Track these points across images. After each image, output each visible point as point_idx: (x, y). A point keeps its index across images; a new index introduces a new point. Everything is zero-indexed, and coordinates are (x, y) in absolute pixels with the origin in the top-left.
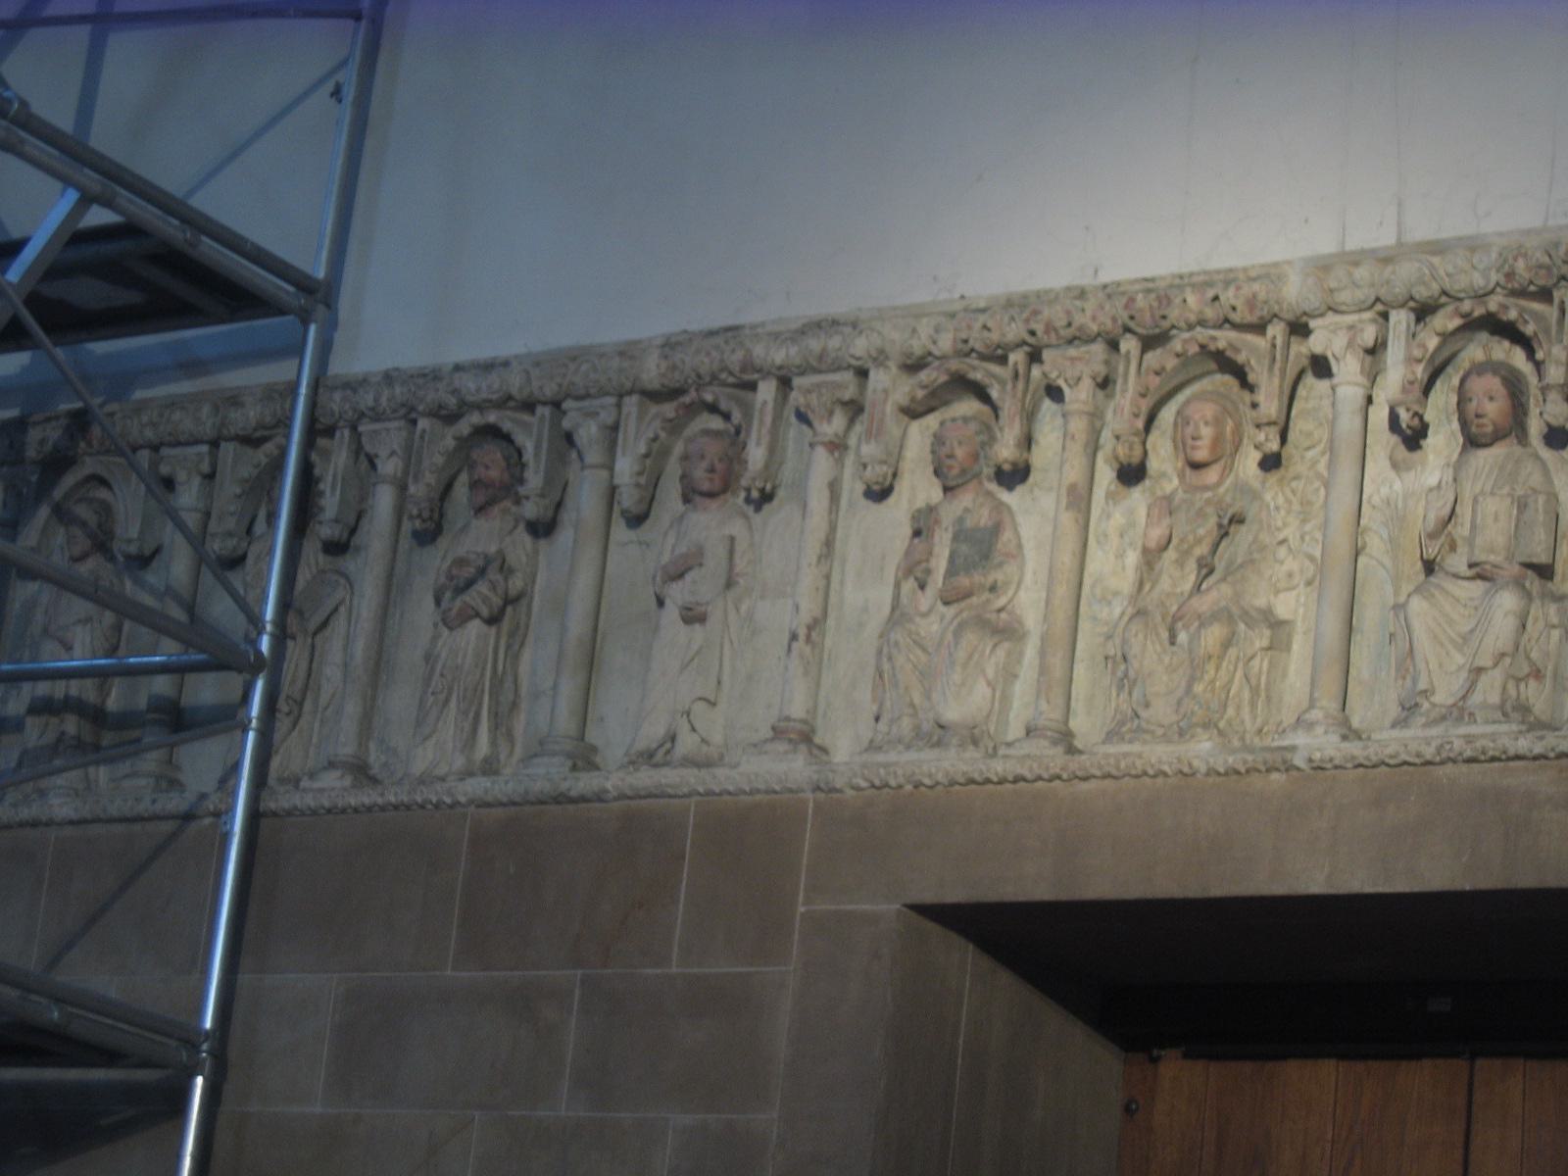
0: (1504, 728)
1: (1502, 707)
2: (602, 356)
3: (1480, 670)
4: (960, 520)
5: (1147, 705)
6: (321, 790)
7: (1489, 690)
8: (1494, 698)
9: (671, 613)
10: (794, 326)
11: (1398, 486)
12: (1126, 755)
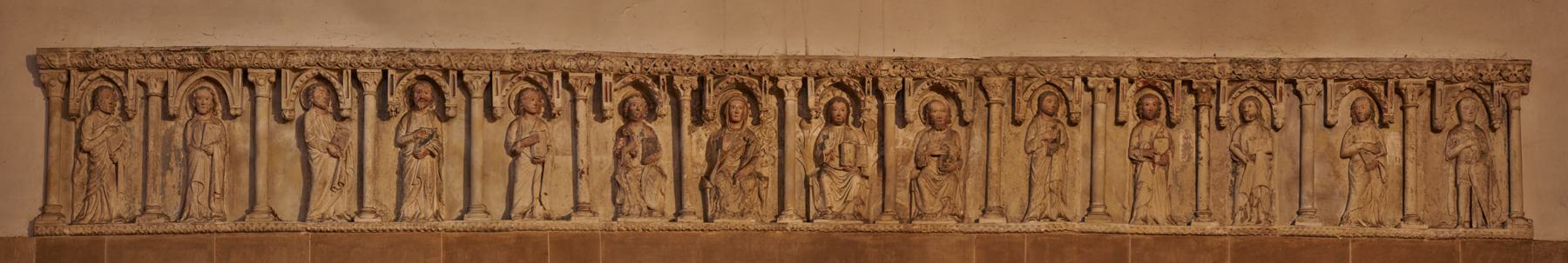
0: (857, 222)
1: (853, 215)
2: (484, 54)
3: (848, 202)
4: (642, 134)
5: (728, 206)
6: (368, 223)
7: (850, 209)
8: (851, 212)
9: (525, 159)
10: (575, 54)
11: (802, 134)
12: (724, 223)
